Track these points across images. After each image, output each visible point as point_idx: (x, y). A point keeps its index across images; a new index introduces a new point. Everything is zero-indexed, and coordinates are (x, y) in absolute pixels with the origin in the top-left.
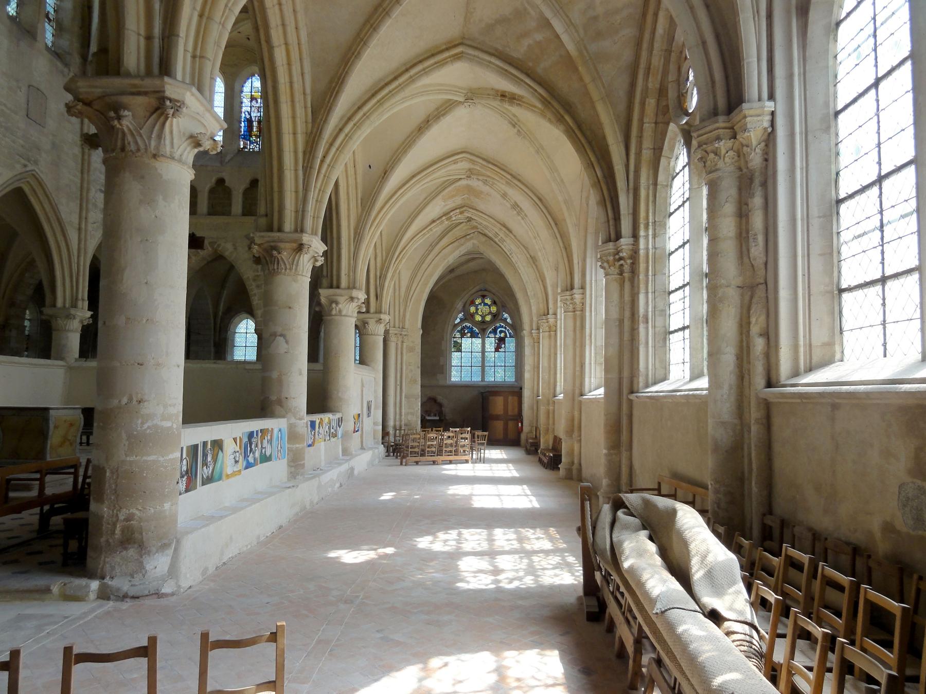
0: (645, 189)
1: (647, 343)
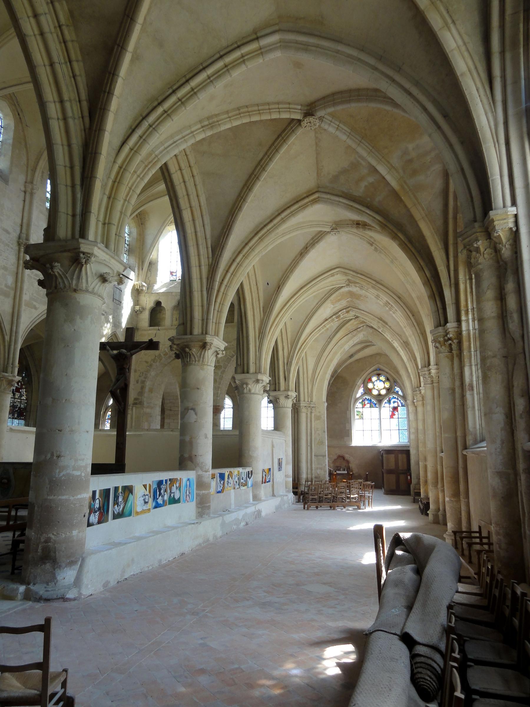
0: (463, 283)
1: (474, 407)
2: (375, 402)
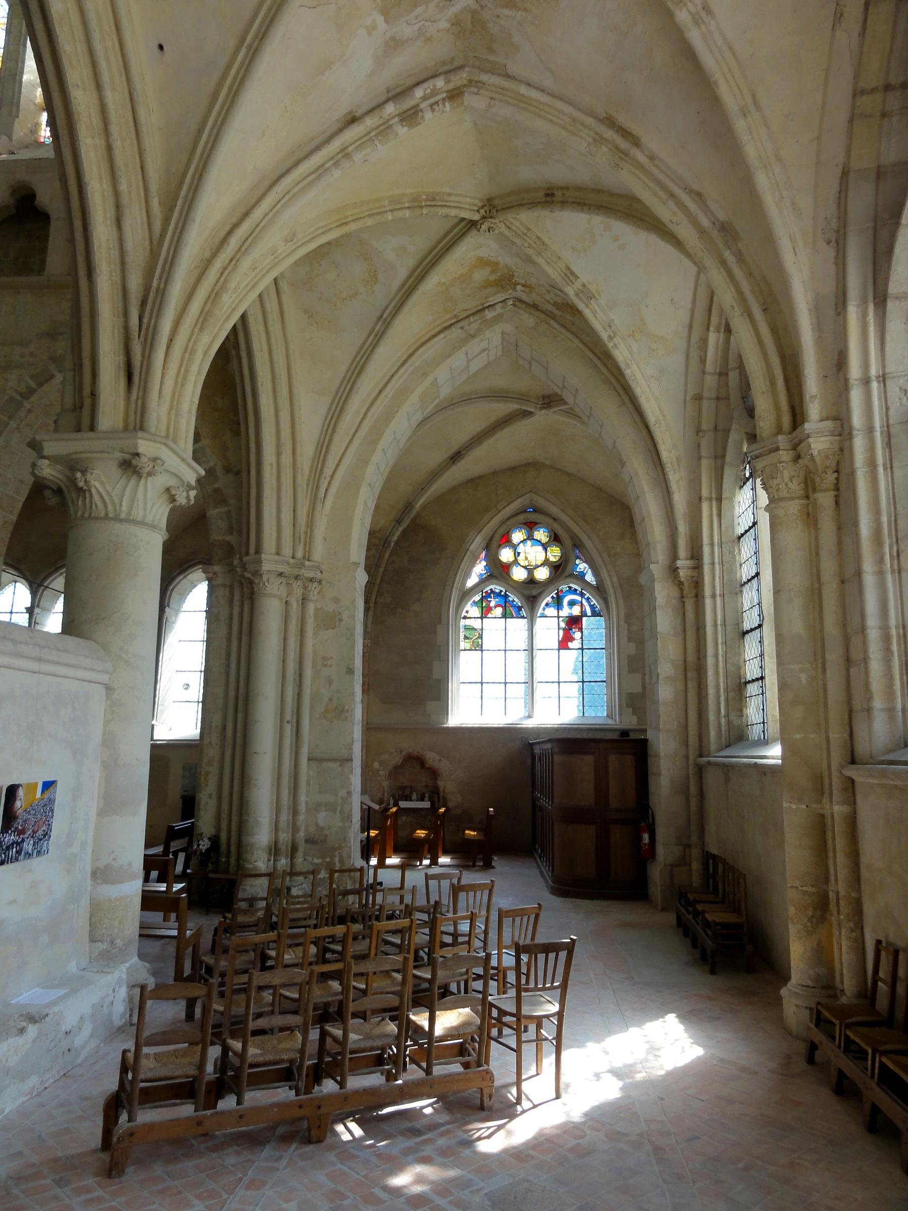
2: (518, 602)
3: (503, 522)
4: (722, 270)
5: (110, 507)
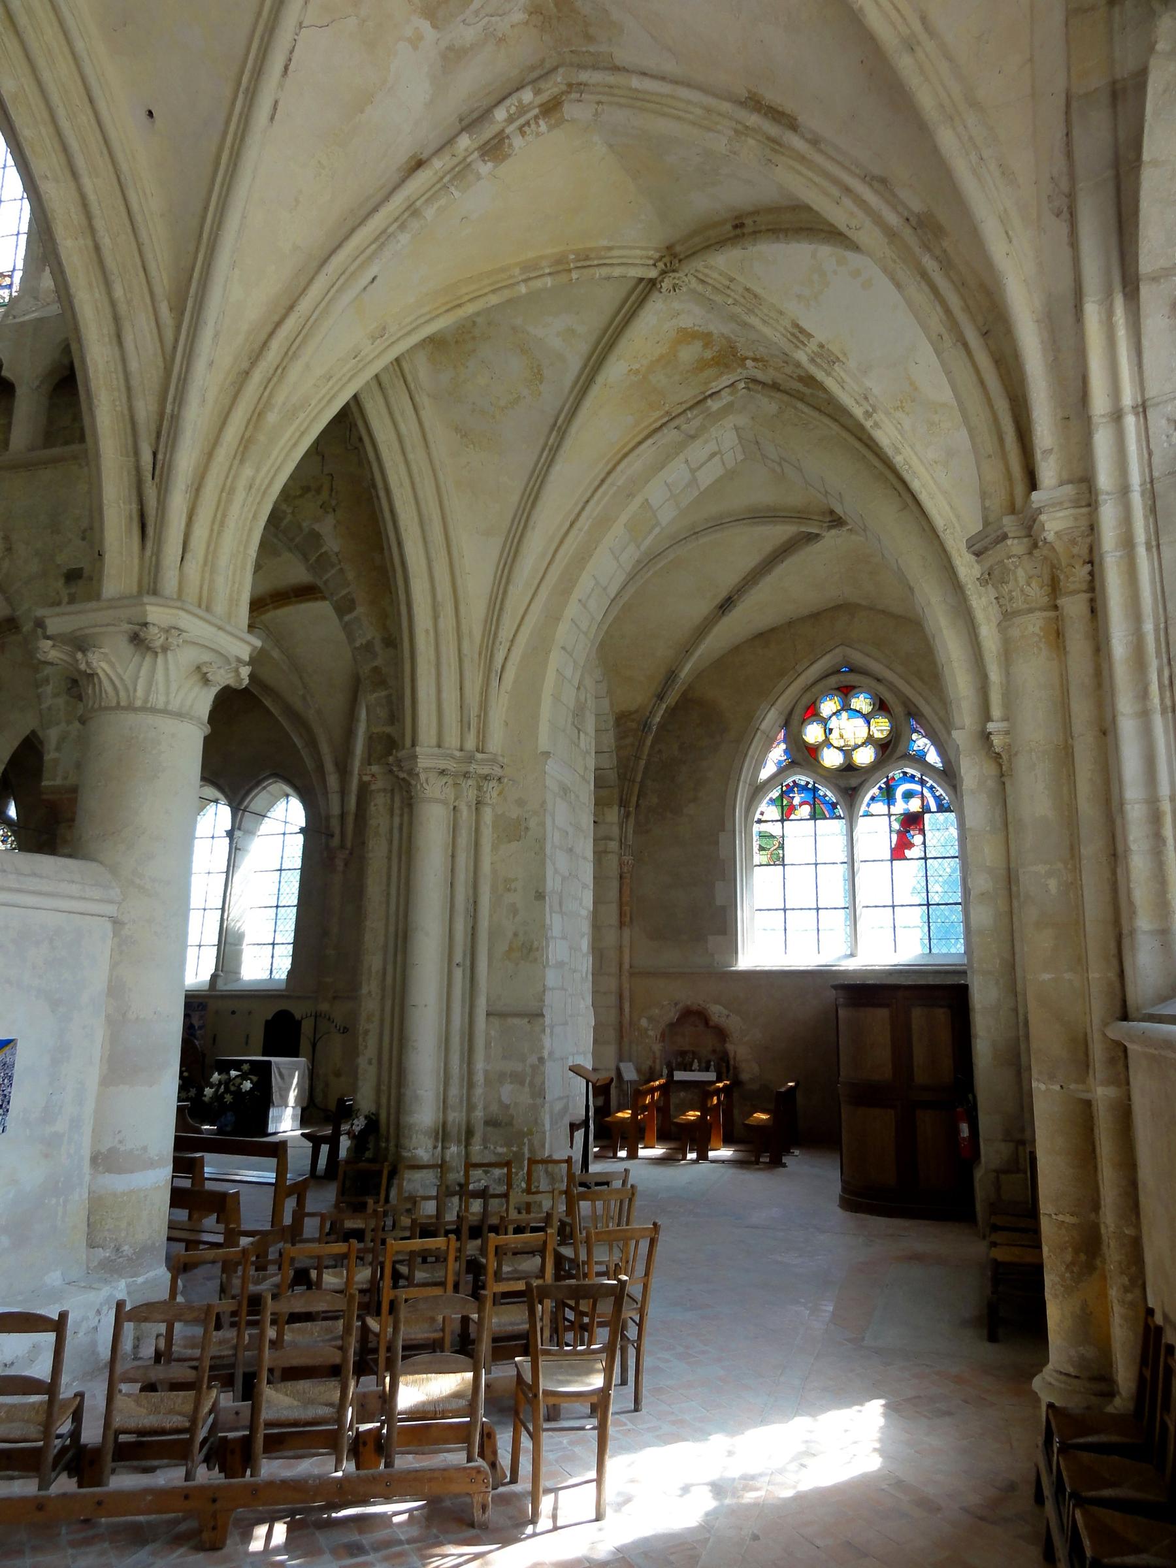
2: (831, 796)
3: (808, 689)
4: (923, 284)
5: (122, 694)
